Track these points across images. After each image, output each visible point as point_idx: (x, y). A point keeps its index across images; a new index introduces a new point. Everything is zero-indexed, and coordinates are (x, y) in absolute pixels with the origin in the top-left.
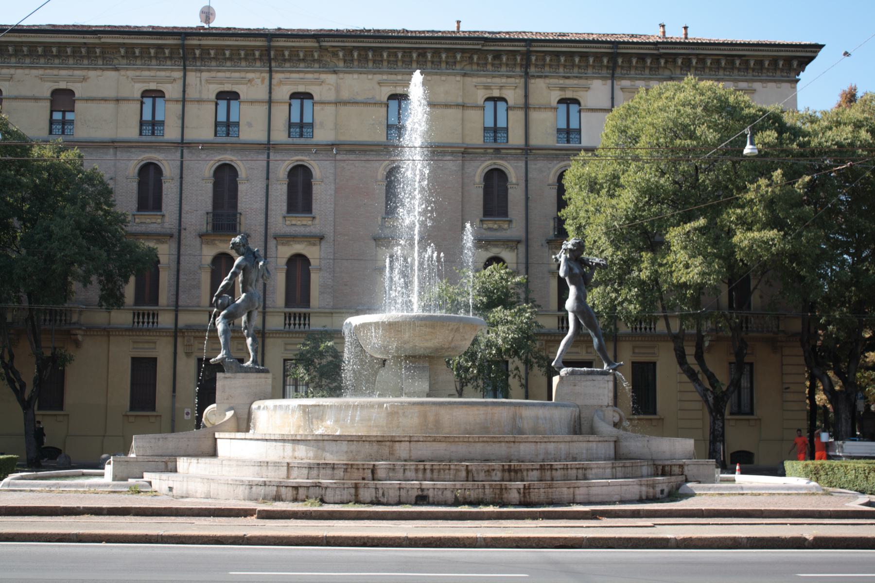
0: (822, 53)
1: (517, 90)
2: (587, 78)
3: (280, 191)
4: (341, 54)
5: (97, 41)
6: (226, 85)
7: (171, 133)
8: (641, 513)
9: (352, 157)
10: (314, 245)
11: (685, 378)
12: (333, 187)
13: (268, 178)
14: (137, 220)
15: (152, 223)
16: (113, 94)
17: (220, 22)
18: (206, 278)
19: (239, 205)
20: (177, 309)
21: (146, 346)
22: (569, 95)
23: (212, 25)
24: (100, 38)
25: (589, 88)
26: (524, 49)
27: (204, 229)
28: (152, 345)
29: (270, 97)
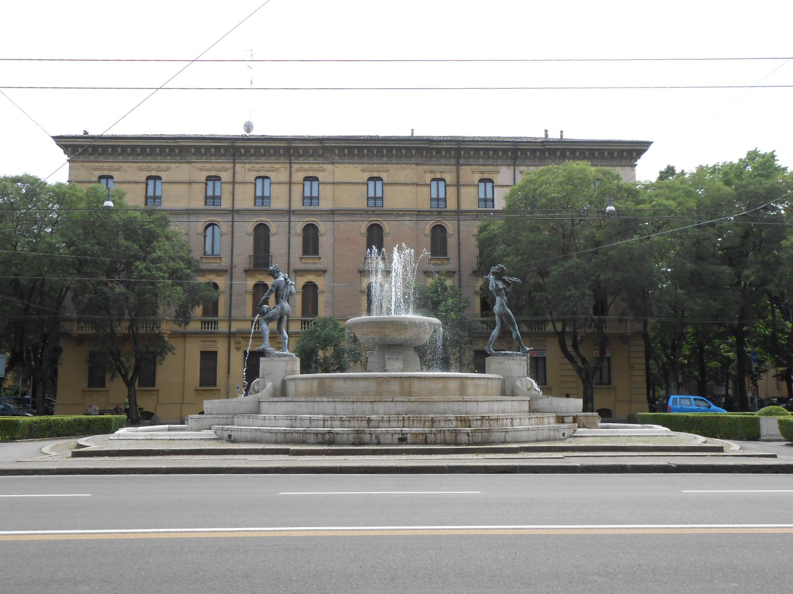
0: (651, 147)
1: (452, 174)
2: (497, 165)
3: (297, 242)
4: (337, 151)
5: (176, 144)
6: (261, 172)
7: (226, 204)
8: (554, 448)
9: (345, 218)
10: (320, 276)
11: (566, 360)
12: (332, 238)
13: (289, 233)
16: (186, 179)
17: (256, 132)
18: (249, 300)
19: (271, 250)
20: (230, 320)
21: (210, 343)
22: (486, 176)
23: (251, 134)
24: (178, 142)
25: (499, 172)
26: (457, 146)
27: (247, 267)
28: (214, 343)
29: (290, 180)
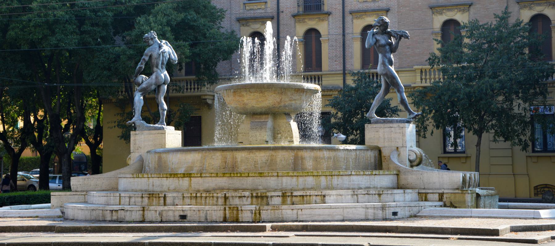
14: (247, 8)
15: (258, 9)
